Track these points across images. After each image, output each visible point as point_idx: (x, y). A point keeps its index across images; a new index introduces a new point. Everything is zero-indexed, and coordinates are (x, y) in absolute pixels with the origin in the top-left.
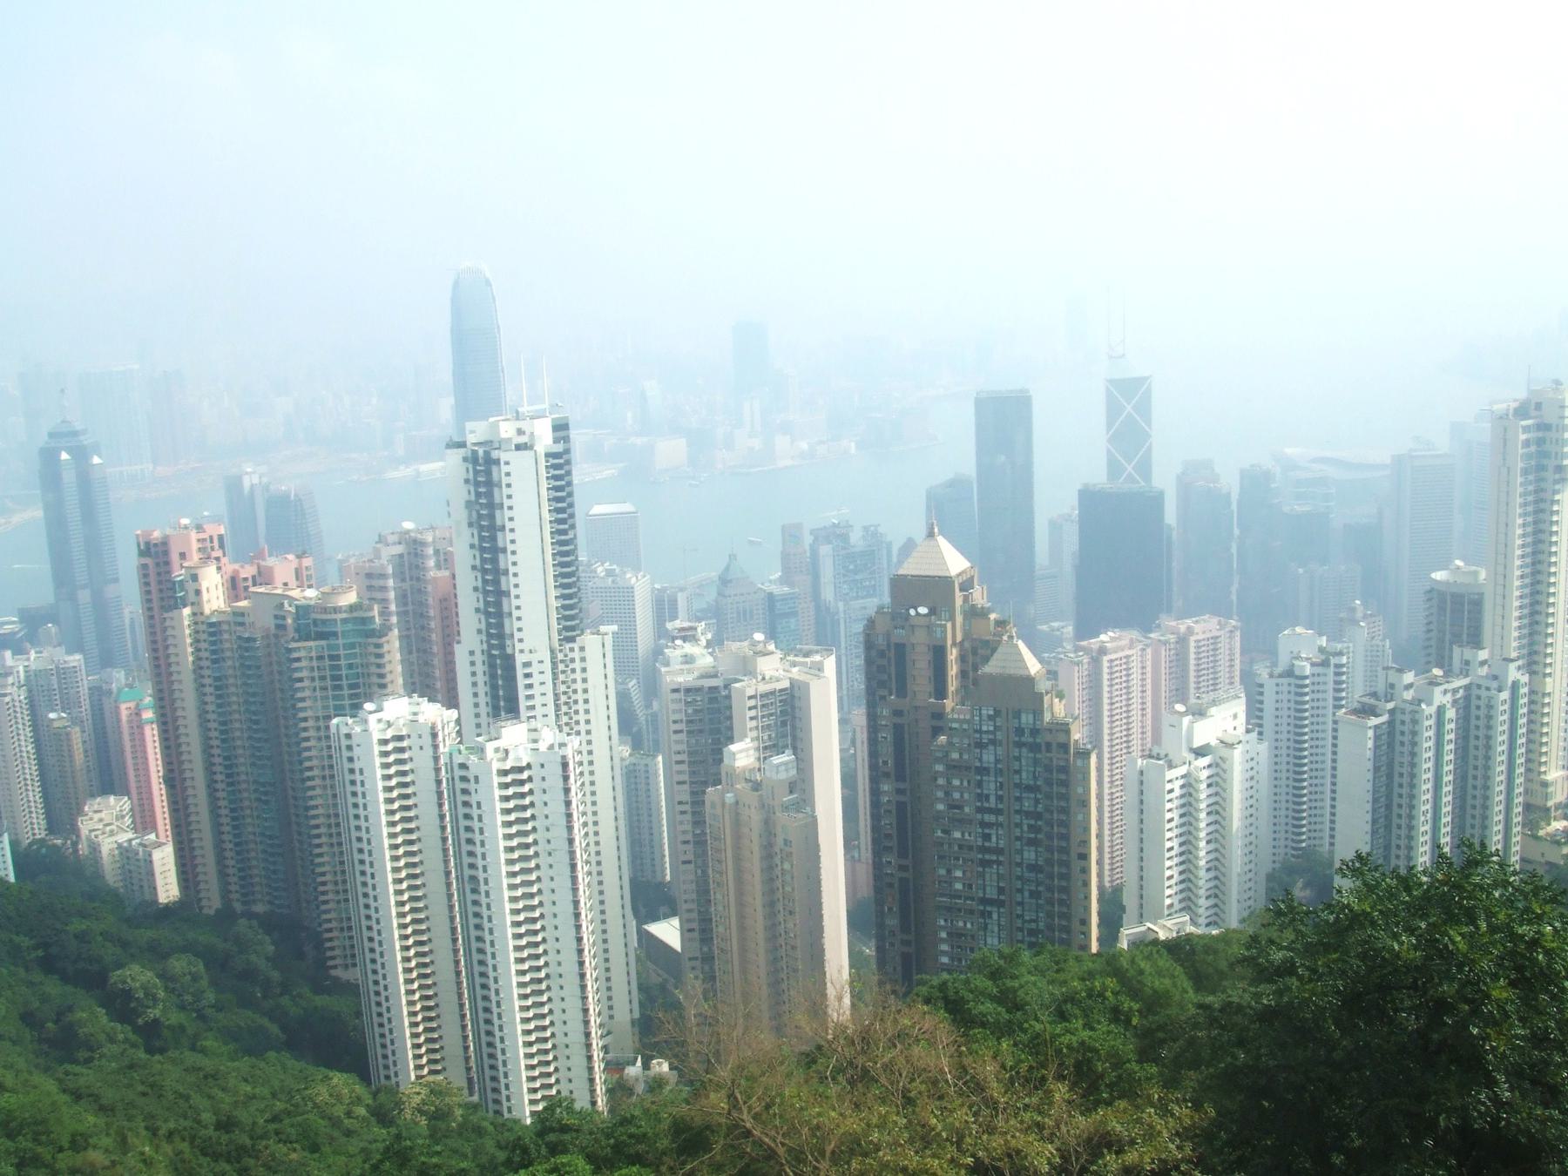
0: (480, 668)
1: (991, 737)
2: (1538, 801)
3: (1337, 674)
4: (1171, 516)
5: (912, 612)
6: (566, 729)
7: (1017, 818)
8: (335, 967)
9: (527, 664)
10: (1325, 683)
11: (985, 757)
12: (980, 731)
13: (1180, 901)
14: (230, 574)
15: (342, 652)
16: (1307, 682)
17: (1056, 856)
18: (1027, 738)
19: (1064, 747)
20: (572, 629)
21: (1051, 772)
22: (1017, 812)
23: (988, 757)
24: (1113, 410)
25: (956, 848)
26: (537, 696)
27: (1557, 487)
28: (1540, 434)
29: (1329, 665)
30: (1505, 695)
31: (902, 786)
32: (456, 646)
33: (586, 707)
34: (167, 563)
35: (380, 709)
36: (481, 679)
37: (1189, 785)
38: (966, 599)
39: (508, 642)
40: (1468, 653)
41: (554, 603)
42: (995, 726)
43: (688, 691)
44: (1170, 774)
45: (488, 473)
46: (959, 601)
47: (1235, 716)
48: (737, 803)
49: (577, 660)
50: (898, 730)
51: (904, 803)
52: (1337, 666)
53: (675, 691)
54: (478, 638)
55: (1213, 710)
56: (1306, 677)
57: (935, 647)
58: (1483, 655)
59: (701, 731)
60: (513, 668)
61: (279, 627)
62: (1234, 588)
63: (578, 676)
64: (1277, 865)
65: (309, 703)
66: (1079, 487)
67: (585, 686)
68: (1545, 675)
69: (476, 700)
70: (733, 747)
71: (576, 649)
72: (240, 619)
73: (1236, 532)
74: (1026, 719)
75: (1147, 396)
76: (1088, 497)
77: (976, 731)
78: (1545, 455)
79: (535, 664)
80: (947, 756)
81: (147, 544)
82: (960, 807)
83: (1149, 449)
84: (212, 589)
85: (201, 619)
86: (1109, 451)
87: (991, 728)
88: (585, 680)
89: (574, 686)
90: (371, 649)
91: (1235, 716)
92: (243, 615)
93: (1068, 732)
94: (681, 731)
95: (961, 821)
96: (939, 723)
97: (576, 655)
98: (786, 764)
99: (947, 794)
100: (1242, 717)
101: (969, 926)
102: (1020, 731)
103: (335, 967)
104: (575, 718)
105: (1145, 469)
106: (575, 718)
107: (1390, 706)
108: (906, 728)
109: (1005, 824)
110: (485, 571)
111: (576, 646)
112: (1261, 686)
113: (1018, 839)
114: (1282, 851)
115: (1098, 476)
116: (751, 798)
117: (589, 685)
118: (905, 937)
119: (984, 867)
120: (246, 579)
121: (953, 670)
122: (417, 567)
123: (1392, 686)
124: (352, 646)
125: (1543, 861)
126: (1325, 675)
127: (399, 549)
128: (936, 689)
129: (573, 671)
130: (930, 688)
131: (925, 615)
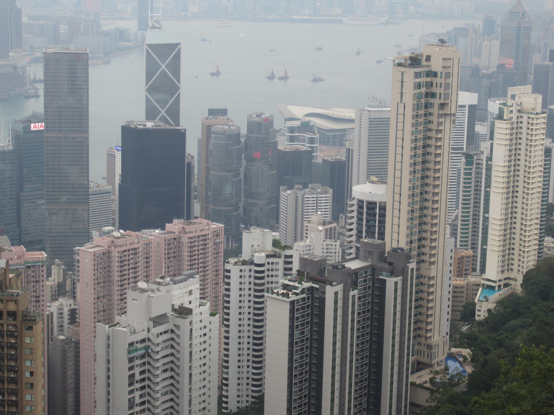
3: (286, 263)
27: (441, 120)
28: (429, 79)
47: (190, 293)
52: (286, 257)
56: (263, 265)
62: (241, 205)
66: (123, 124)
68: (431, 263)
73: (244, 163)
75: (177, 57)
78: (433, 95)
83: (179, 96)
86: (148, 101)
91: (190, 293)
100: (197, 294)
105: (174, 112)
112: (229, 271)
114: (244, 399)
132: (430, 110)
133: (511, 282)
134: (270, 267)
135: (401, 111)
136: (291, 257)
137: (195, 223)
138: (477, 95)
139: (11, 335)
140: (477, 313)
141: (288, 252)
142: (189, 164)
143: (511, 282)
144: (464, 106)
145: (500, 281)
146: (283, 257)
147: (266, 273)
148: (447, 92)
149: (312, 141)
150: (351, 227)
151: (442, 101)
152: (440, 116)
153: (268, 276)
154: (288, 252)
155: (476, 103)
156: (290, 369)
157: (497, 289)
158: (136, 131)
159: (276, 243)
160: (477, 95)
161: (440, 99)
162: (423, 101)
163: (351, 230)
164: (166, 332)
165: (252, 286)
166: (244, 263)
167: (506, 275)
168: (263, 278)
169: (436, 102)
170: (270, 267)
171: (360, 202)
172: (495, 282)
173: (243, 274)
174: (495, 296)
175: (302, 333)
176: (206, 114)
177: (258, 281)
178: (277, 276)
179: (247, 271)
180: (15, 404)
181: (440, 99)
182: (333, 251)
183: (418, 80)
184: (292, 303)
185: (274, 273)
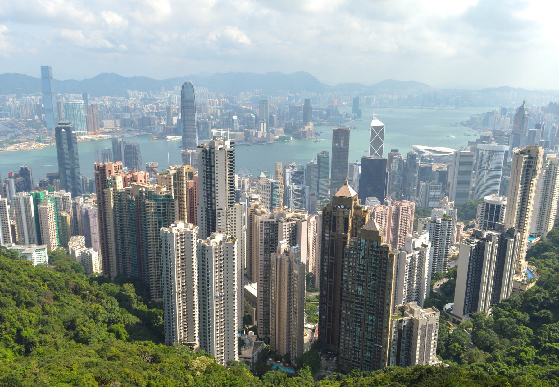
0: (204, 213)
3: (449, 223)
5: (339, 207)
6: (229, 232)
7: (370, 272)
8: (153, 298)
9: (219, 213)
11: (361, 253)
14: (124, 176)
15: (162, 205)
16: (440, 225)
17: (381, 284)
18: (375, 249)
19: (386, 252)
20: (232, 203)
21: (382, 260)
24: (373, 134)
26: (222, 222)
27: (533, 176)
28: (529, 160)
31: (332, 258)
32: (197, 206)
34: (105, 173)
35: (176, 226)
36: (204, 216)
37: (413, 259)
38: (355, 204)
39: (213, 206)
41: (228, 195)
43: (265, 222)
44: (407, 256)
45: (210, 156)
46: (353, 205)
47: (426, 238)
48: (281, 258)
50: (333, 241)
51: (333, 263)
52: (449, 221)
53: (261, 222)
54: (204, 204)
55: (420, 237)
60: (215, 213)
61: (140, 195)
65: (151, 221)
69: (202, 222)
70: (281, 242)
72: (128, 192)
74: (375, 243)
78: (531, 166)
79: (221, 213)
81: (98, 167)
84: (120, 182)
85: (116, 191)
90: (171, 205)
91: (426, 238)
92: (129, 191)
93: (388, 248)
96: (344, 240)
97: (233, 210)
99: (349, 263)
102: (373, 247)
103: (153, 298)
104: (232, 228)
105: (381, 152)
106: (232, 228)
109: (366, 273)
110: (207, 184)
111: (233, 208)
113: (369, 278)
115: (368, 155)
116: (286, 258)
118: (329, 302)
120: (129, 179)
122: (180, 177)
124: (165, 204)
125: (519, 289)
127: (175, 171)
130: (343, 230)
132: (529, 172)
133: (541, 234)
134: (443, 224)
137: (404, 202)
142: (387, 173)
143: (541, 234)
144: (503, 151)
156: (468, 272)
162: (526, 168)
165: (435, 231)
166: (432, 222)
167: (538, 231)
169: (532, 169)
170: (443, 224)
171: (488, 205)
173: (431, 226)
175: (474, 259)
176: (390, 152)
180: (385, 283)
184: (471, 247)
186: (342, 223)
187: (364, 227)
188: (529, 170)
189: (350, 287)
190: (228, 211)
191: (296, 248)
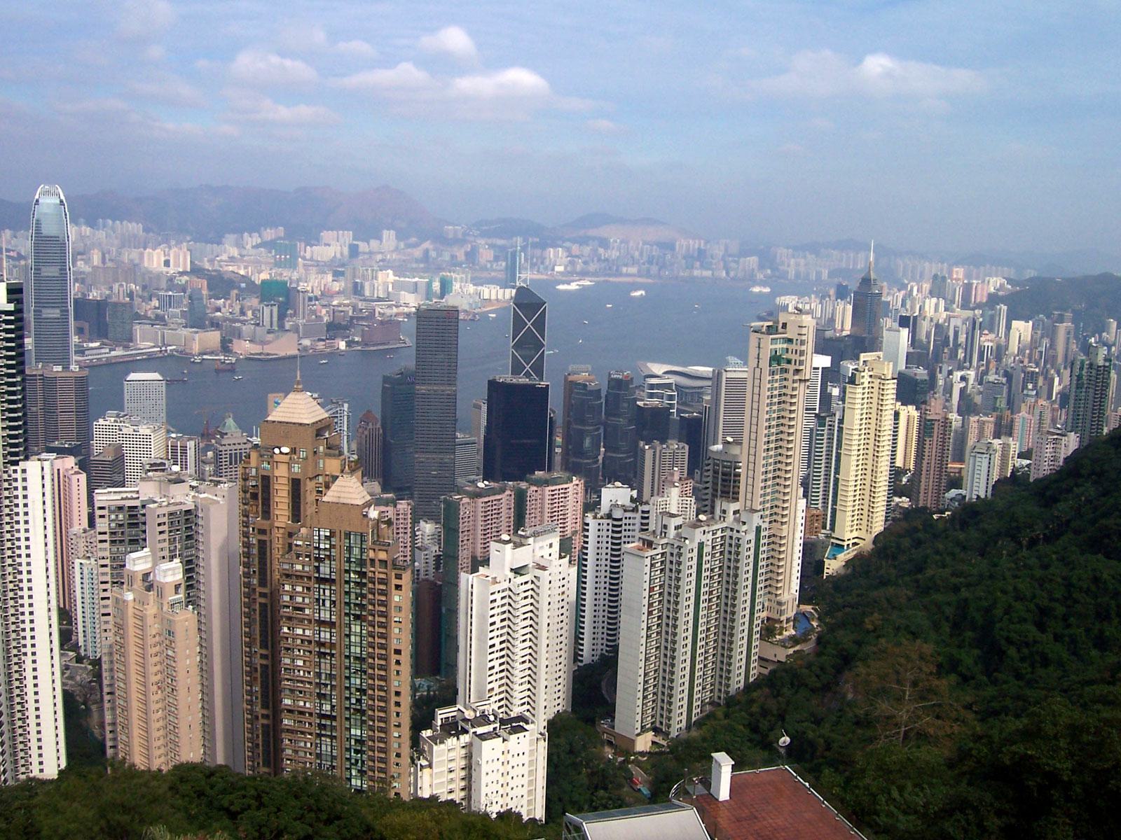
1: (328, 553)
2: (776, 616)
3: (643, 518)
4: (556, 405)
5: (277, 451)
10: (634, 524)
12: (318, 548)
13: (500, 687)
20: (16, 454)
21: (374, 584)
22: (346, 614)
23: (325, 570)
24: (518, 324)
25: (299, 642)
27: (795, 385)
28: (785, 346)
29: (637, 511)
30: (752, 536)
33: (26, 518)
40: (725, 505)
42: (330, 544)
49: (20, 480)
52: (643, 512)
56: (621, 520)
57: (293, 479)
58: (734, 506)
59: (121, 541)
62: (600, 458)
63: (20, 493)
64: (596, 658)
66: (491, 379)
67: (25, 501)
68: (782, 523)
71: (19, 471)
76: (493, 384)
77: (316, 548)
80: (293, 567)
82: (302, 609)
87: (328, 546)
88: (25, 497)
89: (16, 501)
91: (551, 545)
94: (105, 541)
95: (302, 620)
97: (19, 476)
98: (173, 569)
99: (291, 598)
100: (556, 547)
101: (308, 705)
102: (350, 549)
105: (538, 369)
107: (665, 541)
108: (268, 544)
112: (588, 525)
114: (600, 647)
117: (29, 501)
119: (319, 658)
121: (309, 496)
123: (665, 527)
126: (634, 518)
128: (293, 515)
129: (16, 488)
131: (286, 454)
134: (628, 521)
135: (757, 376)
136: (648, 512)
138: (830, 358)
139: (382, 582)
140: (826, 571)
141: (645, 508)
144: (818, 369)
145: (849, 540)
146: (640, 512)
147: (624, 527)
148: (802, 358)
149: (671, 398)
150: (707, 485)
151: (797, 367)
152: (794, 381)
153: (625, 530)
154: (645, 508)
155: (829, 365)
157: (845, 548)
158: (504, 386)
159: (632, 500)
160: (830, 358)
161: (795, 364)
163: (707, 488)
164: (526, 583)
165: (609, 540)
167: (855, 534)
168: (620, 532)
169: (792, 367)
170: (628, 521)
172: (844, 541)
173: (601, 527)
174: (843, 557)
177: (615, 535)
178: (634, 530)
179: (605, 525)
181: (795, 364)
182: (688, 506)
183: (773, 347)
185: (631, 527)
186: (285, 494)
187: (329, 497)
188: (786, 371)
189: (300, 663)
190: (5, 476)
191: (170, 569)
